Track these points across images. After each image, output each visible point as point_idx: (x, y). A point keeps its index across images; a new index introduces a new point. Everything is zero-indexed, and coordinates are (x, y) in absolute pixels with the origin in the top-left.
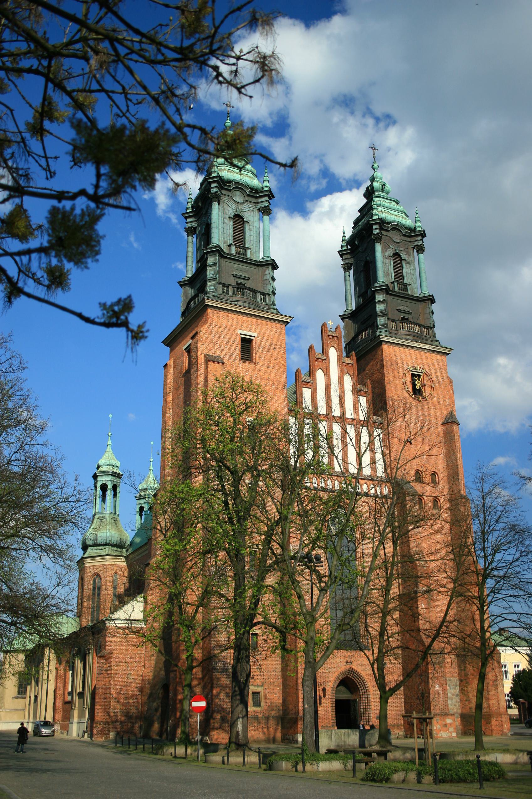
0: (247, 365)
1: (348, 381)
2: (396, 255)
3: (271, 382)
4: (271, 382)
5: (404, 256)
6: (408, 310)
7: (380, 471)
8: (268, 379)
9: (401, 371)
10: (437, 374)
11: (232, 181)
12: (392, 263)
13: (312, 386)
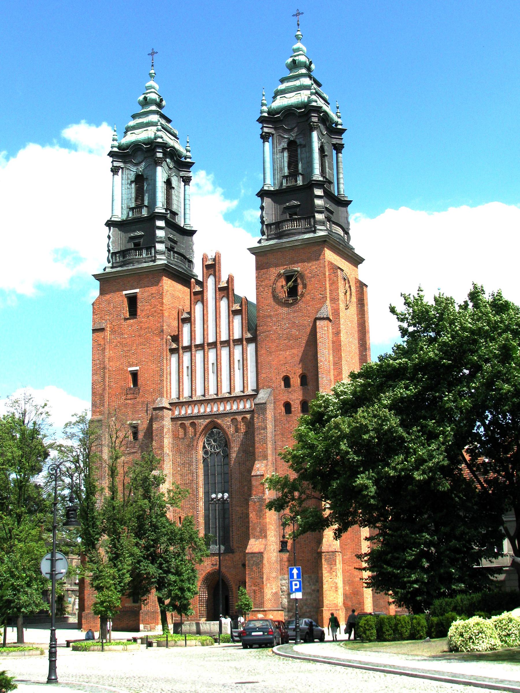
3: (150, 330)
4: (150, 330)
5: (298, 141)
8: (148, 328)
10: (314, 267)
11: (130, 145)
12: (286, 154)
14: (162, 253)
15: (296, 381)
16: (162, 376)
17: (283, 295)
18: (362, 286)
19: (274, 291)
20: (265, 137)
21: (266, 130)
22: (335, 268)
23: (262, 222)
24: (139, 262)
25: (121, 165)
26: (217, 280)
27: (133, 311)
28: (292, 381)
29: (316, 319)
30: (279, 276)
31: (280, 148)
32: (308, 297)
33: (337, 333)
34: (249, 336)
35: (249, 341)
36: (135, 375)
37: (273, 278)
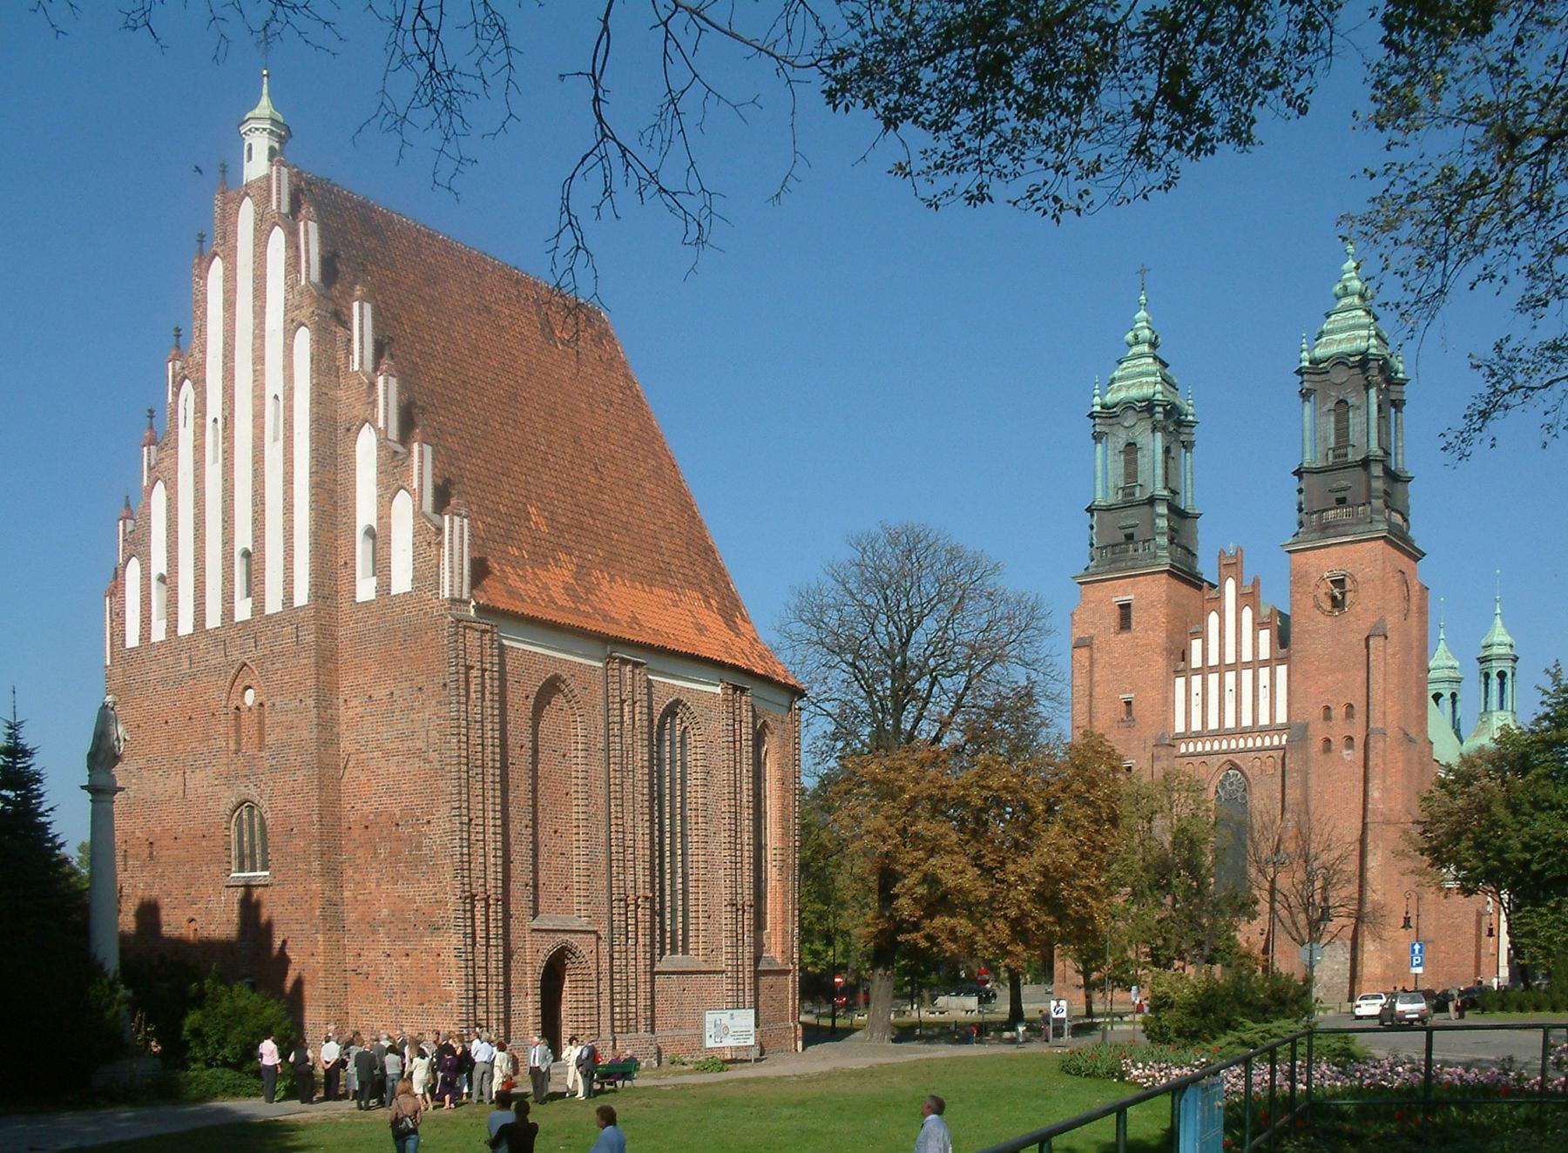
0: (1124, 635)
1: (1247, 614)
2: (1342, 402)
6: (1344, 483)
7: (1281, 718)
9: (1313, 582)
12: (1332, 419)
13: (1202, 634)
15: (1338, 712)
20: (1305, 395)
21: (1306, 385)
23: (1300, 510)
28: (1333, 713)
36: (1128, 703)
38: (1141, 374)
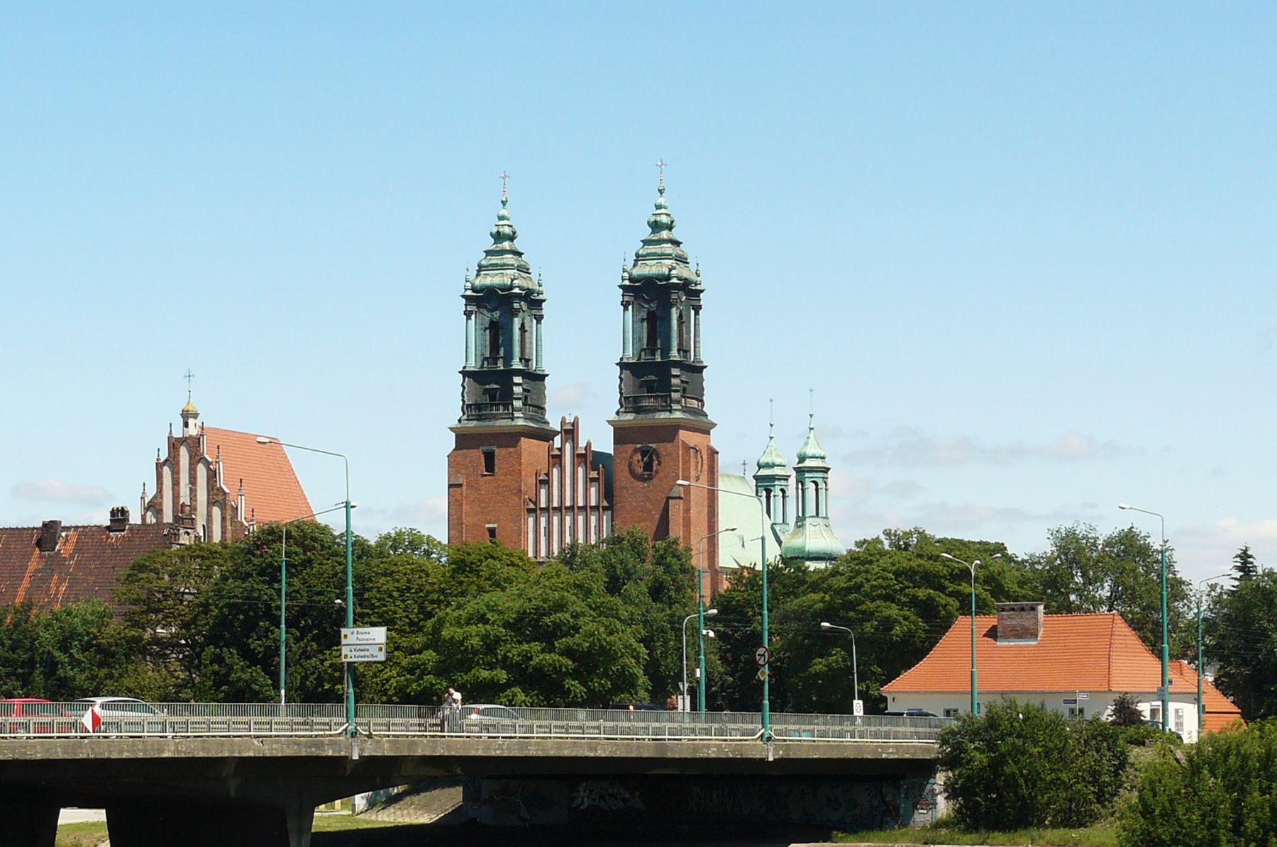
12: (645, 324)
14: (520, 410)
16: (520, 535)
17: (639, 470)
18: (713, 453)
19: (630, 465)
22: (687, 448)
24: (495, 417)
25: (474, 308)
26: (574, 447)
27: (490, 466)
29: (669, 498)
30: (636, 451)
31: (640, 317)
32: (661, 475)
33: (688, 510)
34: (606, 504)
35: (605, 509)
36: (492, 532)
37: (630, 452)
38: (504, 267)
